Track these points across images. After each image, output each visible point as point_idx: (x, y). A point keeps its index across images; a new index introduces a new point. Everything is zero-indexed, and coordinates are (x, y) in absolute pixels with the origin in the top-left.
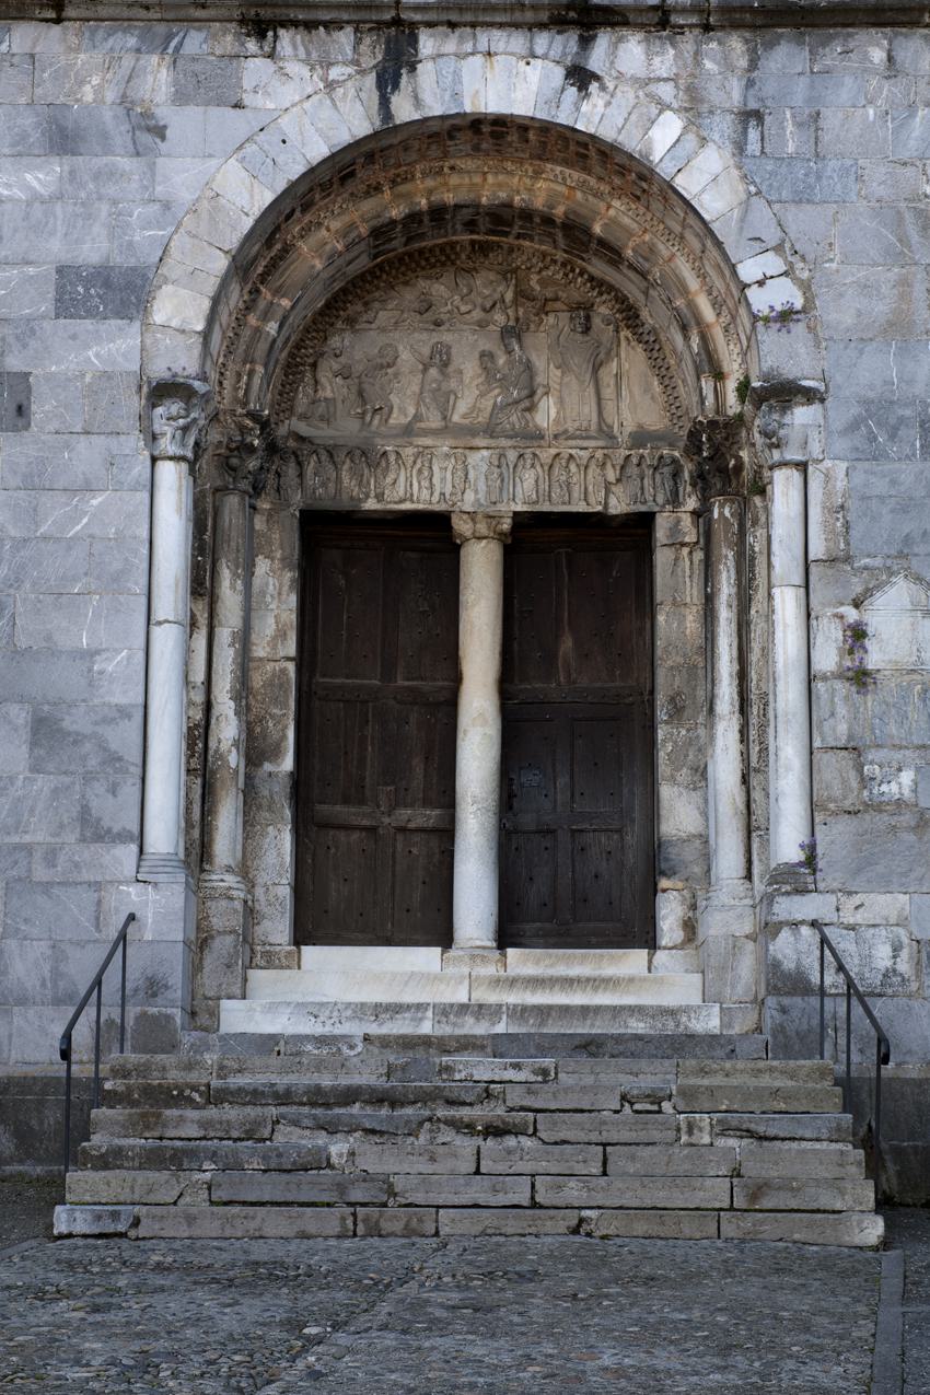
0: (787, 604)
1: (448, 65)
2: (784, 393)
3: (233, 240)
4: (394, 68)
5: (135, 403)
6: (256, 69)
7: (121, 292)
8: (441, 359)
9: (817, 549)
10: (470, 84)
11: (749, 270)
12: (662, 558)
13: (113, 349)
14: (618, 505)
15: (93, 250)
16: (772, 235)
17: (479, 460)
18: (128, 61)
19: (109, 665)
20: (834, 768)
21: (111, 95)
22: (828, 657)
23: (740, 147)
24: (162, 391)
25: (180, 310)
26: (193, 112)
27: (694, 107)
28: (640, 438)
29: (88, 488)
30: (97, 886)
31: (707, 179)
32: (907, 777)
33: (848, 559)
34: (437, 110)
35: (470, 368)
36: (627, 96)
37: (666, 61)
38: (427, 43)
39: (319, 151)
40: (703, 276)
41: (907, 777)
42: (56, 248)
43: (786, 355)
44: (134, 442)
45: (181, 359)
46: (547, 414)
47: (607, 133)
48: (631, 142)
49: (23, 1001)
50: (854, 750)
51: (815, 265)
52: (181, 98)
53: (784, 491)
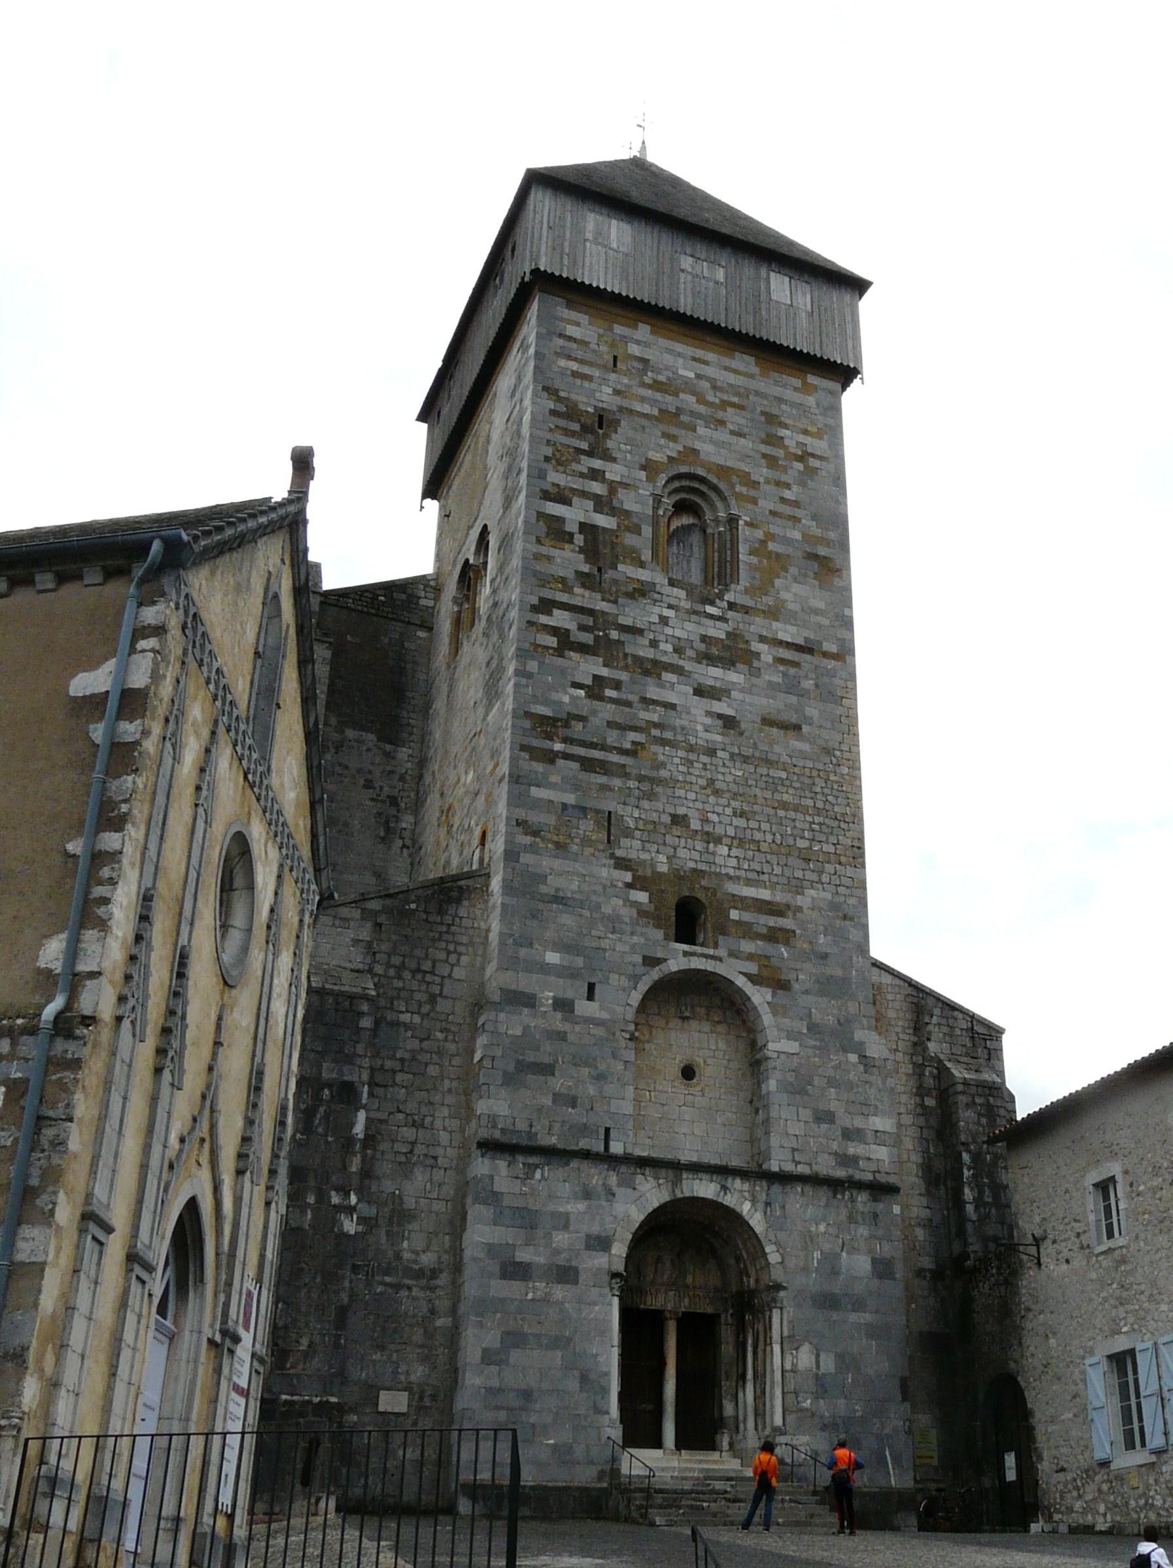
0: (777, 1348)
1: (690, 1182)
2: (778, 1287)
3: (633, 1230)
4: (676, 1182)
5: (607, 1278)
6: (639, 1178)
7: (602, 1243)
8: (659, 1260)
9: (786, 1333)
10: (695, 1188)
11: (767, 1250)
12: (723, 1328)
13: (600, 1261)
14: (710, 1310)
15: (596, 1229)
16: (774, 1240)
17: (671, 1293)
18: (605, 1172)
19: (601, 1359)
20: (791, 1398)
21: (600, 1182)
22: (788, 1366)
23: (765, 1213)
24: (615, 1275)
25: (620, 1249)
26: (623, 1189)
27: (754, 1201)
28: (716, 1290)
29: (595, 1304)
30: (598, 1428)
31: (757, 1222)
32: (809, 1401)
33: (793, 1336)
34: (687, 1195)
35: (668, 1264)
36: (736, 1195)
37: (746, 1186)
38: (685, 1176)
39: (656, 1205)
40: (744, 1243)
41: (809, 1401)
42: (585, 1228)
43: (777, 1275)
44: (607, 1290)
45: (620, 1267)
46: (689, 1279)
47: (732, 1206)
48: (738, 1210)
49: (578, 1463)
50: (796, 1393)
51: (785, 1249)
52: (619, 1185)
53: (776, 1314)
